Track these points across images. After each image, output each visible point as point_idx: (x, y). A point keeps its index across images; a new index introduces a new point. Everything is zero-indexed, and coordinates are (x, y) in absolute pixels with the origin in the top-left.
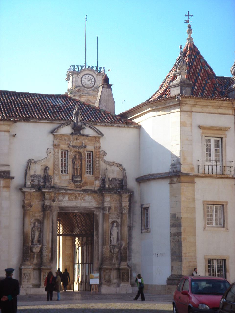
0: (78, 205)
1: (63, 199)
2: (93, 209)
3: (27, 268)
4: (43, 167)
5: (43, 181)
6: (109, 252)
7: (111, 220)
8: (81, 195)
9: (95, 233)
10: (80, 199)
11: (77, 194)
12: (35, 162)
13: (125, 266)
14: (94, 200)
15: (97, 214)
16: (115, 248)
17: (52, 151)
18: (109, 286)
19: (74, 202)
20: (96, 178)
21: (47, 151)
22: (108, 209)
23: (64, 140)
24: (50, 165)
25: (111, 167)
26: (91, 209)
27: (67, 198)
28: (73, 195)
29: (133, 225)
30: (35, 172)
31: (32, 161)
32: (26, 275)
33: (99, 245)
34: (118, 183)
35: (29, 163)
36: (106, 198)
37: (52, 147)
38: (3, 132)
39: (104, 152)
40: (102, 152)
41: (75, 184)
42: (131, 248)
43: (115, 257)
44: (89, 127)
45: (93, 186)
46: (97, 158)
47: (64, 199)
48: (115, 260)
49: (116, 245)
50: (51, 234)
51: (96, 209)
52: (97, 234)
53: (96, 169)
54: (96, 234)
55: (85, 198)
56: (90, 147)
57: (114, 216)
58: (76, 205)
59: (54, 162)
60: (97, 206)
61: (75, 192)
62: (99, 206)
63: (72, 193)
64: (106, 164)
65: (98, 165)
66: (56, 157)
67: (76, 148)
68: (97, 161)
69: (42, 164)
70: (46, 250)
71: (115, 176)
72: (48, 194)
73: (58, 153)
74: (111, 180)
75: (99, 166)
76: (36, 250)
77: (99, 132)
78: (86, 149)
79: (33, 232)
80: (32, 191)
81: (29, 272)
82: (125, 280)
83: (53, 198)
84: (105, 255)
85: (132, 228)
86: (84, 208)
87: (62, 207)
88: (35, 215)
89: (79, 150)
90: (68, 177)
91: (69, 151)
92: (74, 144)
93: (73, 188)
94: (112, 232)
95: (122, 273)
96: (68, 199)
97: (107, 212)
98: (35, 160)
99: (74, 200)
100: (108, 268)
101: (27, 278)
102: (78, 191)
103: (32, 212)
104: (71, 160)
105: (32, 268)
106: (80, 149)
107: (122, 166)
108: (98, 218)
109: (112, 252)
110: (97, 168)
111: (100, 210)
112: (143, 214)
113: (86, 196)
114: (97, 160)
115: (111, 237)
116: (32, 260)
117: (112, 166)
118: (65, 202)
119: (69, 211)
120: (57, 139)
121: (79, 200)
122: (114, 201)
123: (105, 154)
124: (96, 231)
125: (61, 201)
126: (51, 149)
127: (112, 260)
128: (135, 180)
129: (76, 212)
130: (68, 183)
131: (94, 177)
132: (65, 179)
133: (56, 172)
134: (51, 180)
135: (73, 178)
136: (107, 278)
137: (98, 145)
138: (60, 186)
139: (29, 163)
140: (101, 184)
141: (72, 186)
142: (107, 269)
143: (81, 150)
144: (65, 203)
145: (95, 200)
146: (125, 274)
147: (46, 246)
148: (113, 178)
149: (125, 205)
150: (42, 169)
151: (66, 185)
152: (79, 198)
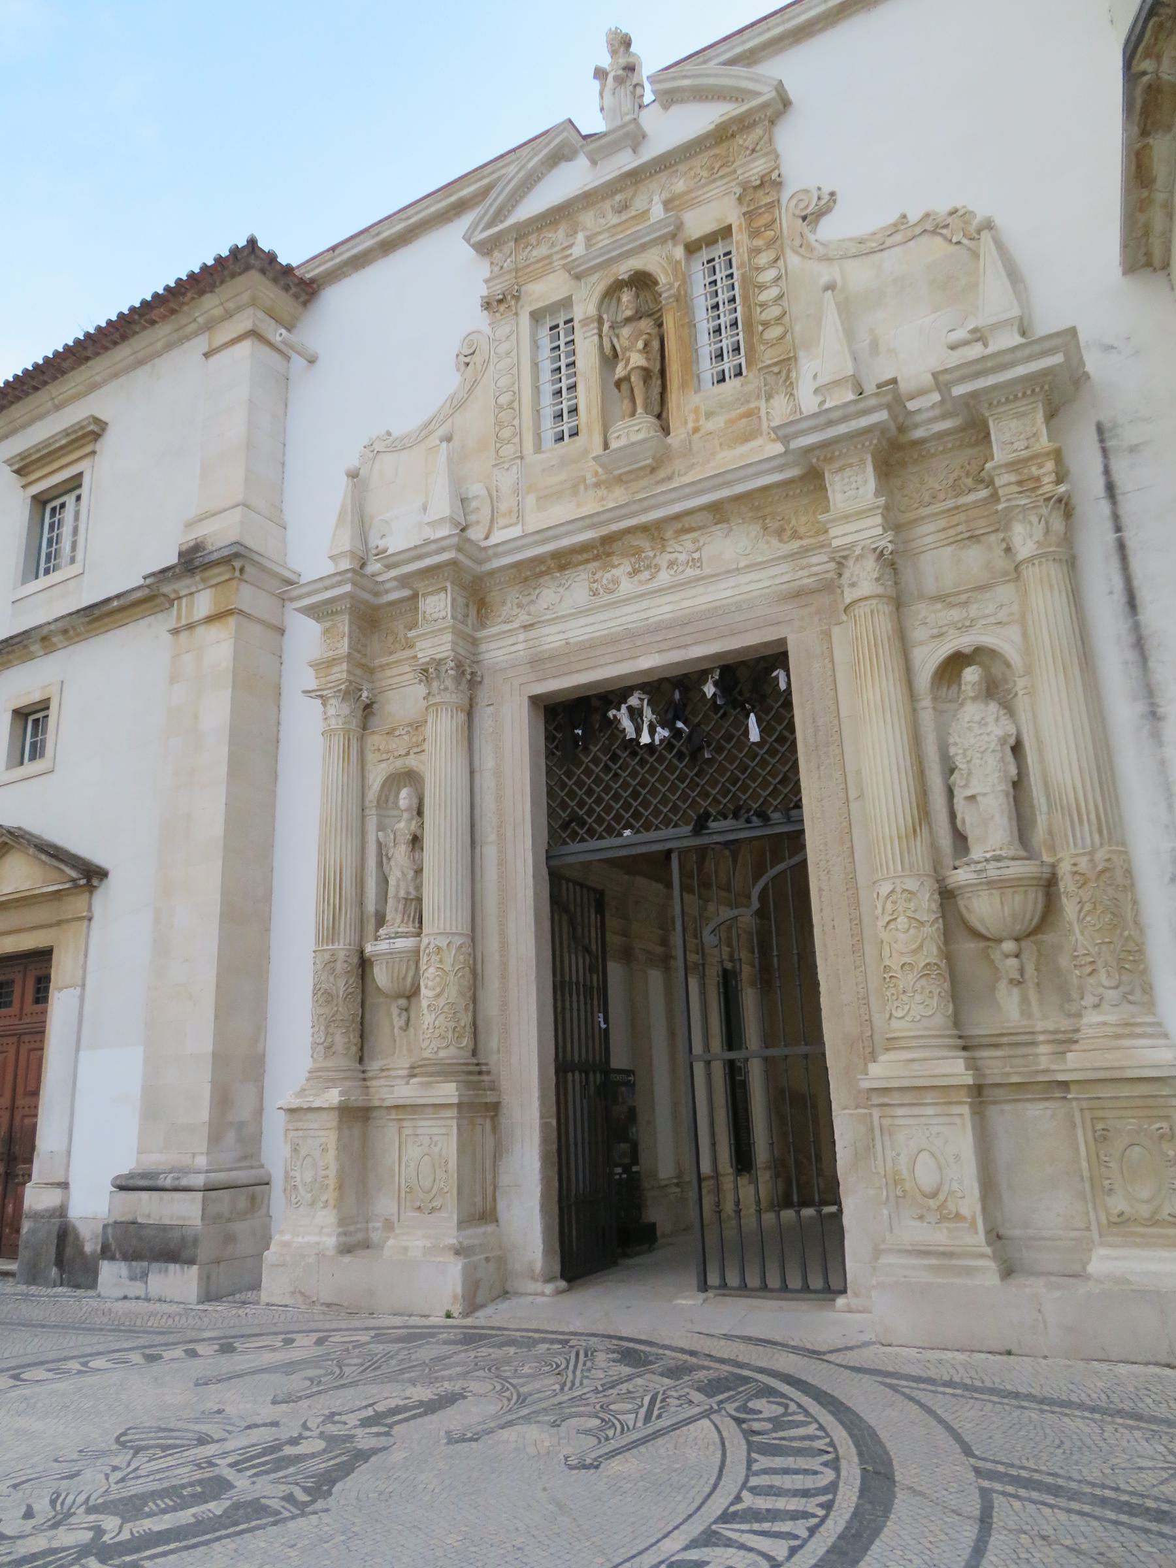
14: (774, 542)
46: (757, 251)
53: (760, 328)
110: (765, 316)
121: (664, 577)
133: (508, 450)
137: (757, 168)
144: (573, 624)
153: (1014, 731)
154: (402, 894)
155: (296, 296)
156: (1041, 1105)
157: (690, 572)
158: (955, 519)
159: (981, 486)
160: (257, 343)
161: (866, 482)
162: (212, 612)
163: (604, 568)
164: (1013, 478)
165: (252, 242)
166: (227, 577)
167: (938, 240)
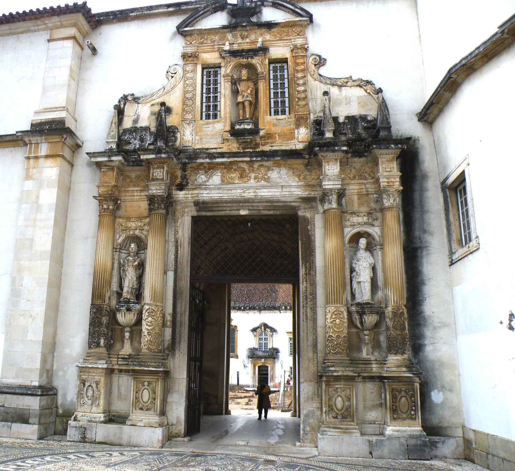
0: (249, 194)
1: (208, 181)
2: (293, 204)
3: (90, 366)
4: (157, 108)
5: (152, 140)
6: (346, 325)
7: (349, 232)
8: (258, 168)
9: (302, 271)
10: (255, 178)
11: (245, 166)
12: (136, 100)
13: (399, 369)
14: (297, 179)
15: (308, 215)
16: (364, 313)
17: (180, 70)
18: (346, 431)
19: (237, 185)
20: (300, 121)
21: (167, 72)
22: (335, 197)
23: (209, 42)
24: (174, 101)
25: (340, 91)
26: (288, 202)
27: (216, 179)
28: (235, 170)
29: (421, 242)
30: (136, 121)
31: (130, 98)
32: (87, 384)
33: (316, 304)
34: (365, 128)
35: (122, 103)
36: (327, 167)
37: (181, 62)
38: (61, 42)
39: (320, 56)
40: (314, 57)
41: (241, 141)
42: (421, 312)
43: (367, 341)
44: (272, 6)
45: (292, 142)
46: (298, 71)
47: (211, 182)
48: (371, 350)
49: (368, 303)
50: (171, 275)
51: (302, 202)
52: (310, 274)
53: (297, 100)
54: (306, 274)
55: (269, 175)
56: (279, 51)
57: (360, 220)
58: (243, 195)
59: (185, 92)
60: (305, 194)
61: (236, 159)
62: (313, 194)
63: (231, 162)
64: (326, 84)
65: (302, 88)
66: (187, 82)
67: (241, 56)
68: (298, 79)
69: (153, 102)
70: (147, 318)
71: (355, 110)
72: (157, 168)
73: (194, 71)
74: (344, 123)
75: (305, 91)
76: (124, 318)
77: (299, 11)
78: (268, 56)
79: (123, 270)
80: (116, 161)
81: (97, 378)
82: (405, 416)
83: (178, 181)
84: (331, 334)
85: (419, 251)
86: (267, 202)
87: (204, 203)
88: (130, 225)
89: (249, 59)
90: (220, 127)
91: (222, 65)
92: (236, 47)
93: (235, 150)
94: (354, 265)
95: (392, 390)
96: (221, 179)
97: (334, 205)
98: (137, 95)
99: (236, 181)
100: (340, 374)
101: (90, 393)
102: (244, 155)
103: (120, 217)
104: (228, 85)
105: (105, 366)
106: (252, 58)
107: (374, 84)
108: (309, 227)
109: (359, 325)
110: (298, 96)
111: (314, 204)
112: (452, 206)
113: (272, 170)
114: (300, 76)
115: (354, 279)
116: (118, 346)
117: (343, 88)
118: (214, 188)
119: (223, 210)
120: (191, 43)
121: (252, 181)
122: (357, 178)
123: (321, 62)
124: (306, 265)
125: (199, 187)
126: (175, 66)
127: (360, 350)
128: (416, 119)
129: (243, 212)
130: (220, 140)
131: (293, 120)
132: (212, 131)
133: (189, 116)
134: (174, 137)
135: (232, 126)
136: (339, 405)
137: (299, 41)
138: (197, 149)
139: (122, 103)
140: (314, 134)
141: (234, 146)
142: (338, 379)
143: (256, 61)
144: (213, 191)
145: (299, 179)
146: (403, 393)
147: (147, 307)
148: (347, 118)
149: (388, 182)
150: (153, 114)
151: (215, 146)
152: (253, 175)
153: (373, 262)
154: (131, 286)
155: (91, 26)
156: (371, 383)
157: (263, 183)
158: (361, 187)
159: (370, 178)
160: (75, 43)
161: (337, 168)
162: (48, 154)
163: (227, 172)
164: (386, 180)
165: (85, 4)
166: (58, 140)
167: (362, 90)
